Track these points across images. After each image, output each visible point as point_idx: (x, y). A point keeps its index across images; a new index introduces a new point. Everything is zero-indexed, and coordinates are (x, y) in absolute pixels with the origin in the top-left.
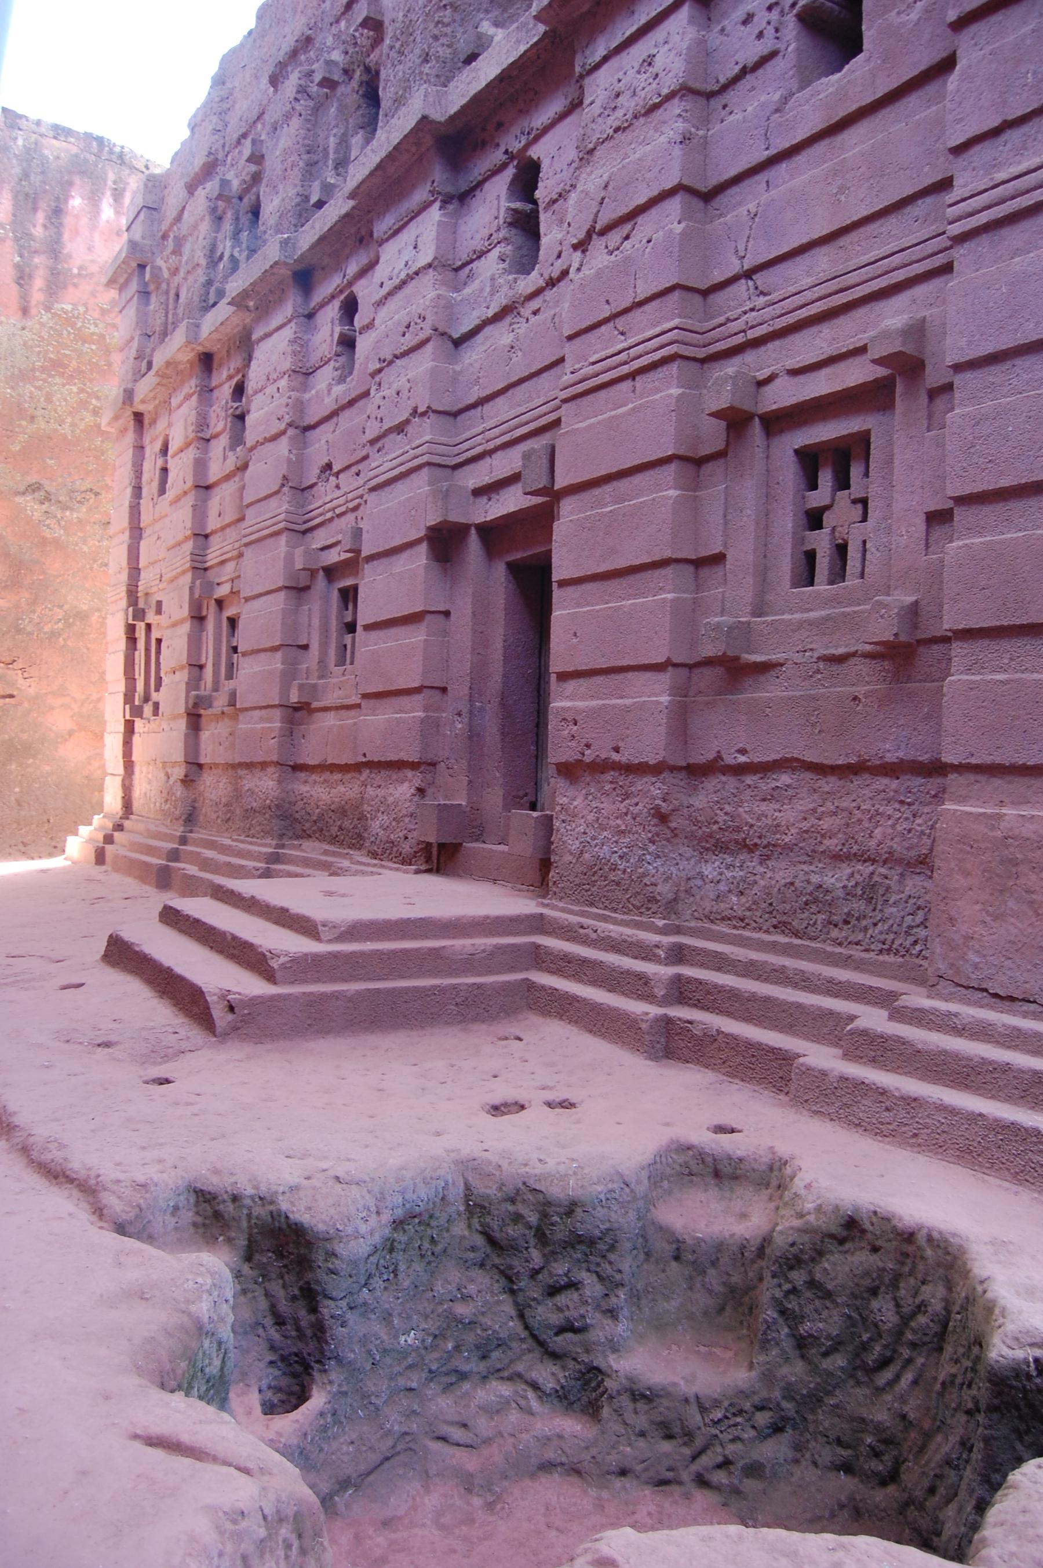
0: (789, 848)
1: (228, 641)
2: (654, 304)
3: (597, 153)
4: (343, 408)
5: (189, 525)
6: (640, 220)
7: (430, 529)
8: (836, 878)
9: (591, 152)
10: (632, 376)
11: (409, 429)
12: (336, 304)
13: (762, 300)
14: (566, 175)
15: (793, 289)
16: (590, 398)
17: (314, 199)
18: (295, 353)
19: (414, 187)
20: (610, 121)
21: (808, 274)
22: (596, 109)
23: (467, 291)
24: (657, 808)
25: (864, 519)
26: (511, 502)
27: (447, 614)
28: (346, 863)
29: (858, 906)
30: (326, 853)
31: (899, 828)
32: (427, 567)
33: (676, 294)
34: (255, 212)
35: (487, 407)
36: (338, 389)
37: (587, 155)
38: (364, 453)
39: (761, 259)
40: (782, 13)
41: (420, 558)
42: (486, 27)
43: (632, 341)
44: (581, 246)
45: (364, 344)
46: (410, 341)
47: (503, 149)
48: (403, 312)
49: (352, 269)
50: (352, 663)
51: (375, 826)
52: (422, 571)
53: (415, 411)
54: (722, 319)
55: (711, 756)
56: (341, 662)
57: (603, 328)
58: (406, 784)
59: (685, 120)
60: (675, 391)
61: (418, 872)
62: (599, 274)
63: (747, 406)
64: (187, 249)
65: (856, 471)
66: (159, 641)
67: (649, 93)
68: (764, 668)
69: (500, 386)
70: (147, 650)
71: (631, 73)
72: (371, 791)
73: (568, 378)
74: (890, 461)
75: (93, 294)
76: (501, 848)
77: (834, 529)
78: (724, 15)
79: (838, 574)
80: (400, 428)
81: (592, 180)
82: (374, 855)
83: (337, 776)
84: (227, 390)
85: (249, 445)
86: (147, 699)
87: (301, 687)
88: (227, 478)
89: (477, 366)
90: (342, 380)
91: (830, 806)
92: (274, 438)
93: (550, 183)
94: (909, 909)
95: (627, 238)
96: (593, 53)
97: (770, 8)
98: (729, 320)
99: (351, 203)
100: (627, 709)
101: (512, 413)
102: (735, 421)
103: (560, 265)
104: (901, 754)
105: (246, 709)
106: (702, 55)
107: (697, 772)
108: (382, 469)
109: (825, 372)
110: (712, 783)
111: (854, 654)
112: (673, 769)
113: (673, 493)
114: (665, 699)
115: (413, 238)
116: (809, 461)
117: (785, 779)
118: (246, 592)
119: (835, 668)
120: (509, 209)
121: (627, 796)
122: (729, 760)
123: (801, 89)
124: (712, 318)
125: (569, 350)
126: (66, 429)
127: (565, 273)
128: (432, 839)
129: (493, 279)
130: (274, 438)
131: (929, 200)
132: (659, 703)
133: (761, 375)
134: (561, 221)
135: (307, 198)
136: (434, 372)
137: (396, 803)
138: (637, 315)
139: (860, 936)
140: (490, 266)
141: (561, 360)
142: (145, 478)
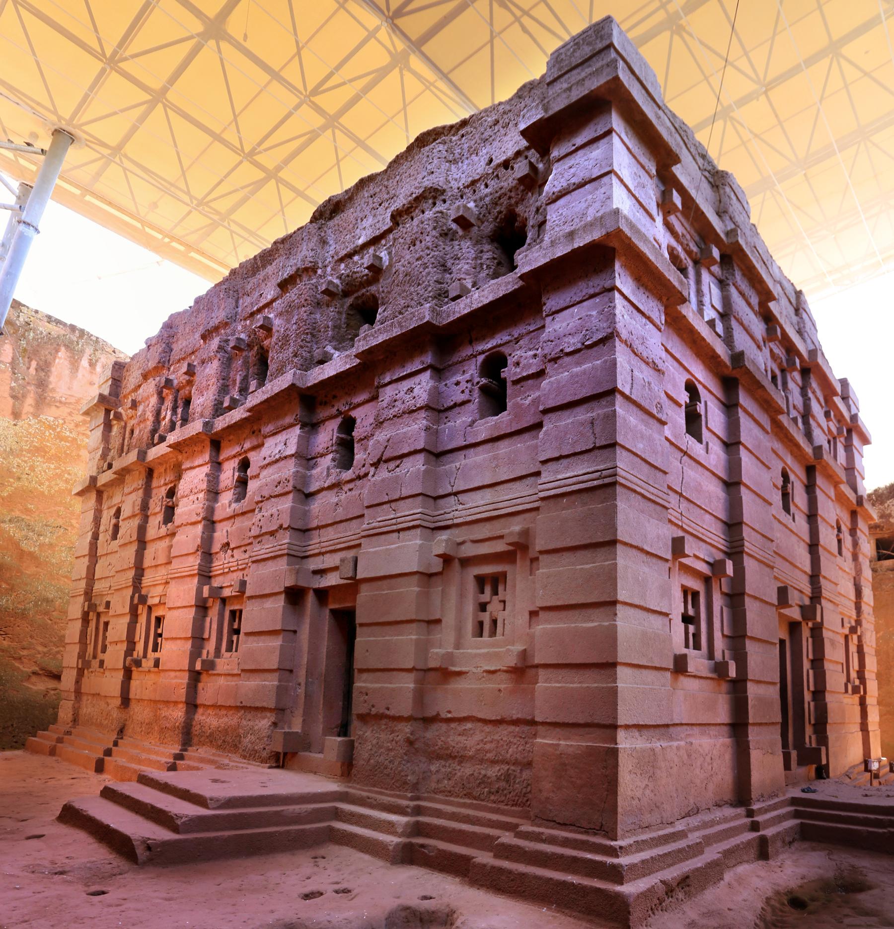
0: (472, 758)
1: (156, 630)
2: (410, 500)
3: (385, 424)
4: (238, 515)
5: (133, 561)
6: (405, 460)
7: (286, 588)
8: (493, 772)
9: (382, 423)
10: (399, 531)
11: (278, 535)
12: (237, 460)
13: (461, 507)
14: (369, 429)
15: (474, 505)
16: (376, 537)
17: (226, 404)
18: (209, 481)
19: (286, 415)
20: (391, 411)
21: (482, 499)
22: (385, 404)
23: (314, 472)
24: (408, 738)
25: (504, 610)
26: (332, 580)
27: (295, 632)
28: (226, 761)
29: (503, 784)
30: (214, 754)
31: (520, 749)
32: (284, 607)
33: (420, 498)
34: (188, 402)
35: (322, 531)
36: (234, 505)
37: (379, 424)
38: (250, 541)
39: (461, 489)
40: (473, 385)
41: (280, 602)
42: (329, 349)
43: (399, 515)
44: (376, 465)
45: (252, 486)
46: (279, 490)
47: (336, 408)
48: (276, 476)
49: (247, 445)
50: (236, 651)
51: (246, 741)
52: (281, 609)
53: (281, 527)
54: (442, 512)
55: (434, 713)
56: (229, 649)
57: (384, 506)
58: (266, 720)
59: (427, 420)
60: (419, 542)
61: (270, 767)
62: (383, 480)
63: (451, 553)
64: (141, 409)
65: (501, 588)
66: (106, 624)
67: (410, 404)
68: (460, 674)
69: (330, 522)
70: (97, 628)
71: (402, 393)
72: (244, 722)
73: (365, 526)
74: (514, 586)
75: (70, 414)
76: (321, 756)
77: (491, 613)
78: (447, 379)
79: (493, 633)
80: (272, 533)
81: (381, 436)
82: (244, 757)
83: (224, 712)
84: (163, 491)
85: (176, 524)
86: (95, 657)
87: (203, 662)
88: (160, 538)
89: (317, 510)
90: (238, 500)
91: (489, 739)
92: (194, 523)
93: (361, 430)
94: (525, 785)
95: (398, 466)
96: (384, 379)
97: (467, 382)
98: (445, 513)
99: (248, 414)
100: (393, 690)
101: (336, 536)
102: (447, 559)
103: (363, 471)
104: (519, 716)
105: (166, 671)
106: (435, 394)
107: (429, 721)
108: (260, 552)
109: (487, 543)
110: (435, 727)
111: (499, 670)
112: (416, 719)
113: (417, 589)
114: (412, 686)
115: (284, 439)
116: (481, 581)
117: (469, 725)
118: (170, 604)
119: (491, 676)
120: (338, 437)
121: (393, 732)
122: (444, 715)
123: (480, 419)
124: (438, 510)
125: (366, 512)
126: (44, 489)
127: (366, 475)
128: (280, 749)
129: (328, 469)
130: (194, 523)
131: (533, 478)
132: (409, 688)
133: (460, 540)
134: (365, 450)
135: (222, 403)
136: (293, 508)
137: (259, 730)
138: (402, 503)
139: (503, 798)
140: (326, 462)
141: (362, 516)
142: (102, 528)
